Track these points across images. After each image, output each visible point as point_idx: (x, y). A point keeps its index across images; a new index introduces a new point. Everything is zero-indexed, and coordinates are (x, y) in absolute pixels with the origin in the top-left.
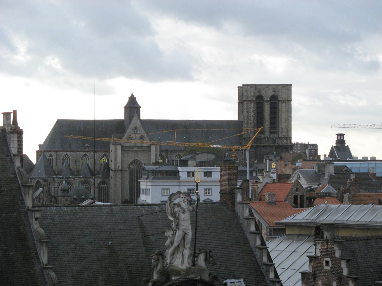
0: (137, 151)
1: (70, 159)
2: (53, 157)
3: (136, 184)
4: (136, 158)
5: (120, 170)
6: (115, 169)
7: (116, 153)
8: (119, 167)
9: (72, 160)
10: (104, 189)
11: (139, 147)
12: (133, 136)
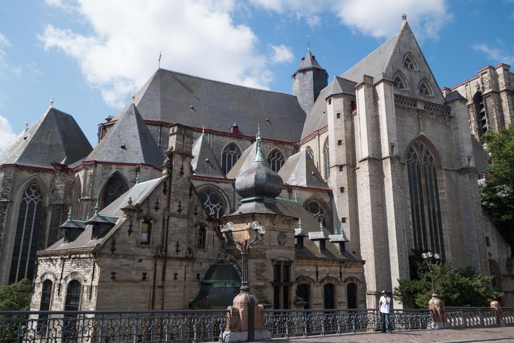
0: (423, 111)
4: (422, 133)
12: (405, 72)
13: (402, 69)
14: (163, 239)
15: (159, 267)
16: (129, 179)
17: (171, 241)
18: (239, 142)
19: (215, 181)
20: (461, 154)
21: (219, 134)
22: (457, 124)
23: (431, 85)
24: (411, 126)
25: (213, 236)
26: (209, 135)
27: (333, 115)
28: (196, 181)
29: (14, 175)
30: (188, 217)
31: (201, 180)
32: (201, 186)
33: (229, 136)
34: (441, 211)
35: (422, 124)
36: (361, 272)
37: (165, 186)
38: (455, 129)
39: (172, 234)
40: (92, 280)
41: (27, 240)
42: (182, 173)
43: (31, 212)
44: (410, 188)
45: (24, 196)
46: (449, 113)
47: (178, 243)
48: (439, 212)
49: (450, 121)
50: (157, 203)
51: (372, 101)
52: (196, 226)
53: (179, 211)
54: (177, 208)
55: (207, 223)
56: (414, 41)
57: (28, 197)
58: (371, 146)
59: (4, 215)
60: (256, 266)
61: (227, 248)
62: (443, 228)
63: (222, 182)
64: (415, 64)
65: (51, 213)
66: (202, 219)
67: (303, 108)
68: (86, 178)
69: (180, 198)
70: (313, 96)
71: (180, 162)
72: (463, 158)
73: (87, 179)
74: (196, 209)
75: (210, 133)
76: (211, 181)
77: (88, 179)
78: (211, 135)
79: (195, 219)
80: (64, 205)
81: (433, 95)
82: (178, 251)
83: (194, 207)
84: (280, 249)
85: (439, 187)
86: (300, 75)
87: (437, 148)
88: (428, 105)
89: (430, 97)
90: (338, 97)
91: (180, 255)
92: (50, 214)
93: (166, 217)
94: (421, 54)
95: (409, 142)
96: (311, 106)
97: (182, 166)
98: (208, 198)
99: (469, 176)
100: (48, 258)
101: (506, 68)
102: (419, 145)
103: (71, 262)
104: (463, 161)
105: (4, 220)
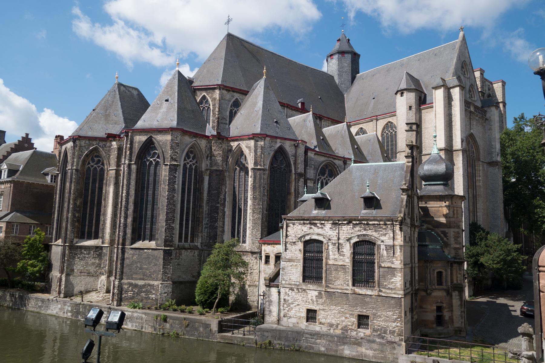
0: (473, 113)
4: (472, 131)
6: (448, 148)
13: (460, 74)
15: (413, 232)
20: (493, 150)
21: (294, 109)
22: (491, 125)
26: (286, 108)
27: (405, 107)
29: (181, 140)
32: (325, 161)
34: (477, 194)
35: (472, 124)
38: (489, 129)
40: (394, 241)
41: (188, 201)
43: (190, 175)
45: (185, 160)
46: (485, 116)
48: (476, 195)
49: (485, 122)
51: (447, 102)
56: (467, 51)
57: (188, 161)
59: (175, 177)
60: (454, 233)
61: (423, 219)
62: (478, 207)
63: (337, 159)
64: (467, 71)
65: (208, 177)
67: (340, 89)
68: (257, 149)
70: (350, 78)
72: (494, 154)
73: (258, 150)
75: (287, 107)
76: (330, 157)
77: (259, 150)
80: (222, 170)
81: (476, 99)
85: (477, 175)
86: (338, 56)
88: (476, 107)
89: (474, 101)
90: (411, 92)
92: (206, 179)
96: (348, 88)
99: (498, 168)
100: (308, 222)
101: (482, 73)
103: (352, 227)
104: (493, 156)
105: (176, 182)
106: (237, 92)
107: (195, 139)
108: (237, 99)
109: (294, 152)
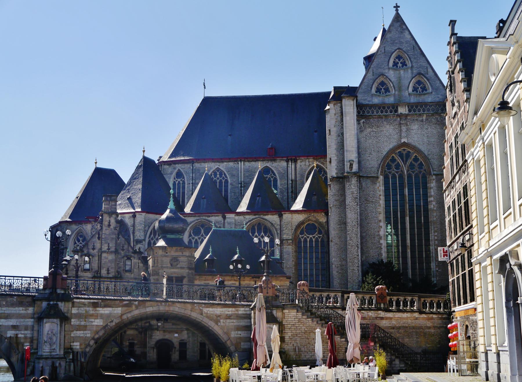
0: (406, 116)
1: (227, 182)
2: (184, 178)
3: (407, 219)
4: (403, 141)
5: (355, 174)
6: (340, 175)
7: (342, 128)
8: (351, 165)
9: (231, 184)
10: (311, 246)
11: (412, 107)
12: (391, 74)
14: (98, 267)
16: (129, 224)
17: (104, 268)
18: (273, 165)
19: (206, 216)
23: (428, 80)
24: (390, 135)
25: (139, 263)
26: (240, 163)
28: (189, 218)
30: (116, 252)
31: (194, 216)
32: (194, 221)
33: (261, 161)
36: (286, 285)
37: (99, 235)
39: (104, 264)
42: (109, 225)
44: (387, 200)
45: (75, 243)
47: (108, 268)
50: (94, 246)
51: (339, 119)
52: (123, 257)
53: (109, 249)
54: (107, 247)
55: (133, 255)
57: (78, 243)
58: (336, 165)
63: (212, 216)
66: (128, 253)
69: (109, 241)
71: (108, 219)
74: (123, 247)
78: (242, 162)
79: (123, 253)
82: (108, 273)
83: (122, 245)
84: (173, 269)
85: (428, 195)
87: (426, 153)
91: (110, 276)
93: (100, 254)
94: (416, 46)
95: (385, 153)
97: (110, 221)
98: (202, 231)
102: (404, 153)
106: (178, 163)
107: (81, 226)
108: (179, 170)
109: (133, 223)
